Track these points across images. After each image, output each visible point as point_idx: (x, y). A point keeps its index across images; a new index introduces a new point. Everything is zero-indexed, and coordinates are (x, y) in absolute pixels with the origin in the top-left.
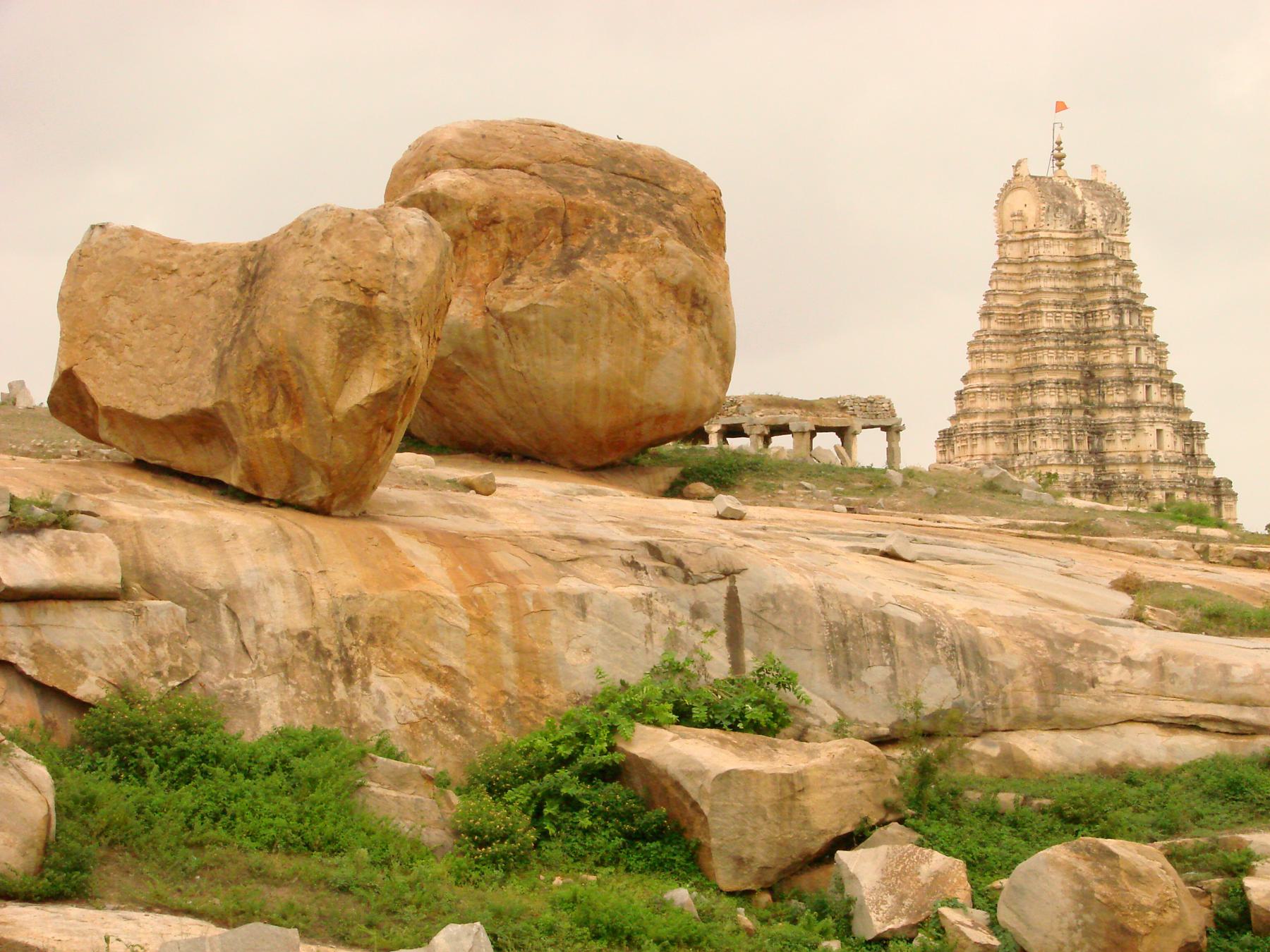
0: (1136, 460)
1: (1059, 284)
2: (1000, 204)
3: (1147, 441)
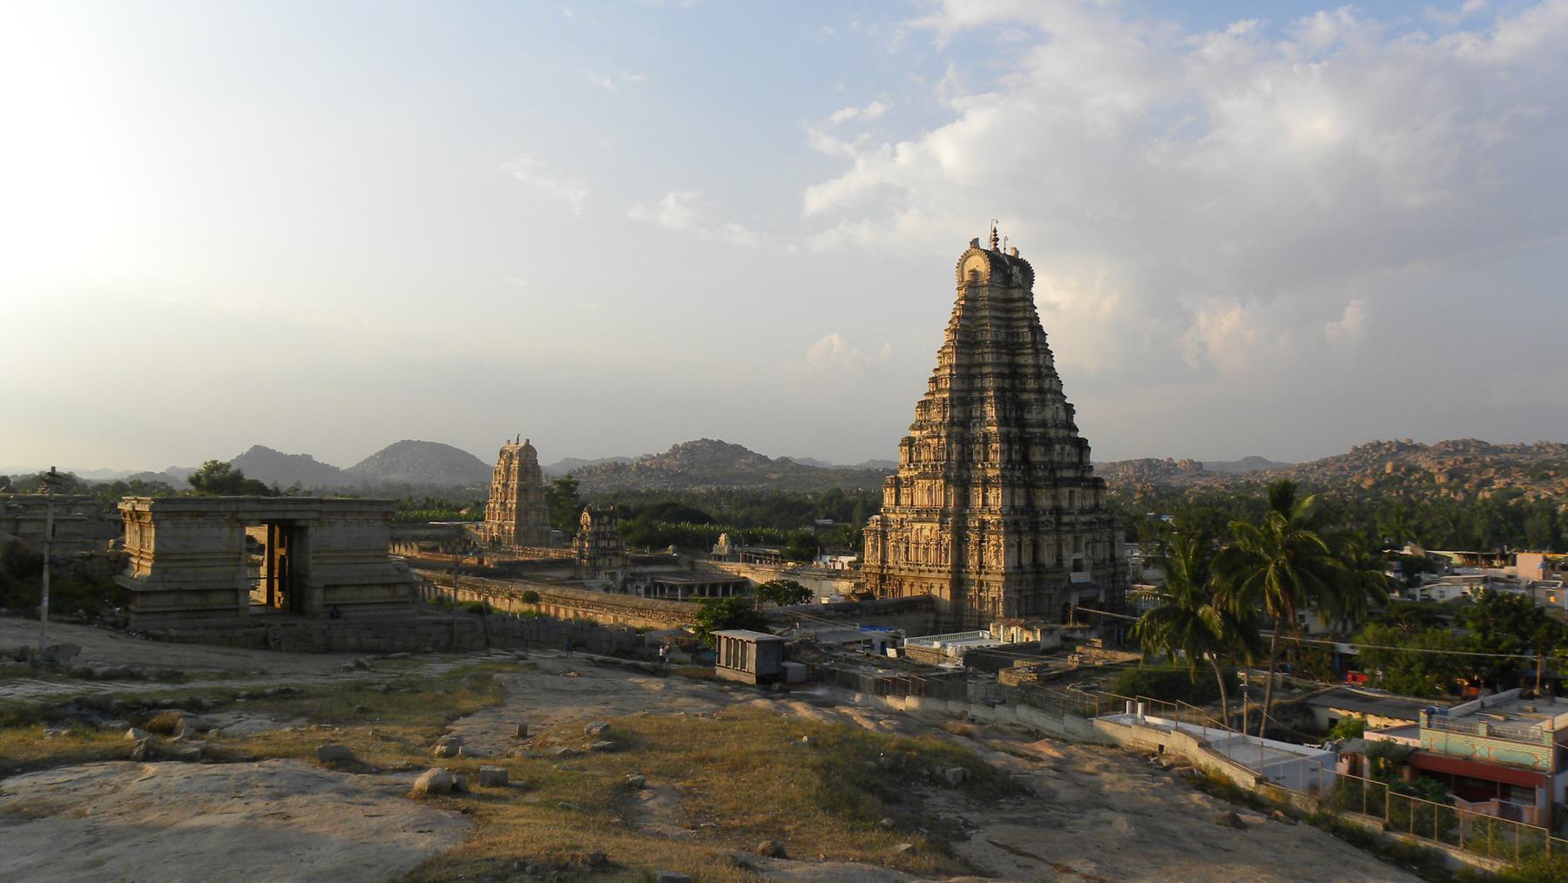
0: (1043, 424)
1: (998, 314)
2: (961, 264)
3: (1049, 413)
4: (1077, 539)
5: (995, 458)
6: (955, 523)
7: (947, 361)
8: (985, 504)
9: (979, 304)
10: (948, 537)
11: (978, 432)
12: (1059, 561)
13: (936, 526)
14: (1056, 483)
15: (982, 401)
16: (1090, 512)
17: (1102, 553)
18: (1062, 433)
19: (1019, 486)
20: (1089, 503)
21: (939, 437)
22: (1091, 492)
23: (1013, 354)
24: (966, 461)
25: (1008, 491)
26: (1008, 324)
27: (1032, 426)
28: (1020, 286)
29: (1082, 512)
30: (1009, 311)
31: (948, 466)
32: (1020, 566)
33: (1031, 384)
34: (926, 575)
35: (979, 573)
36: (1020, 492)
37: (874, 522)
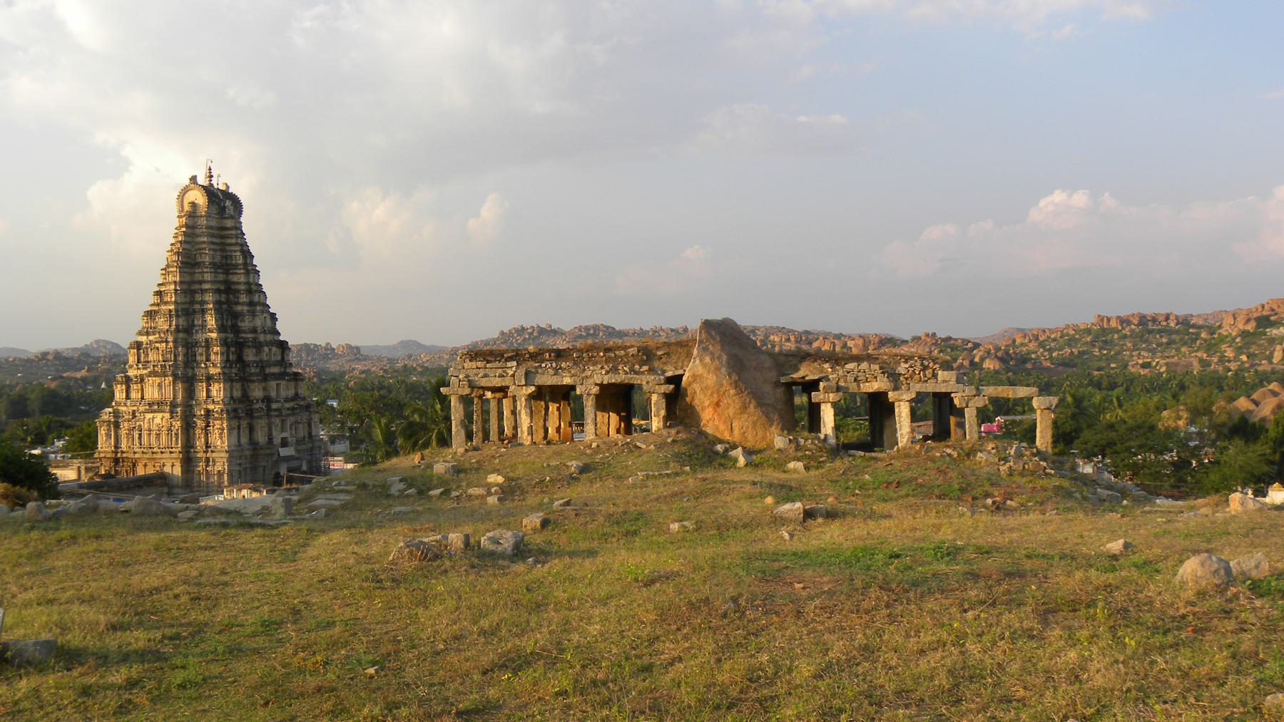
0: (254, 330)
1: (214, 240)
4: (283, 421)
5: (217, 358)
6: (184, 412)
7: (171, 278)
8: (208, 396)
9: (198, 231)
10: (177, 424)
11: (200, 337)
12: (270, 440)
13: (167, 415)
14: (266, 378)
15: (203, 312)
16: (293, 399)
17: (302, 432)
18: (269, 337)
19: (237, 381)
20: (291, 393)
21: (167, 342)
22: (292, 384)
23: (227, 273)
24: (190, 361)
25: (228, 385)
26: (223, 247)
27: (244, 332)
28: (232, 217)
29: (287, 400)
30: (222, 237)
31: (175, 366)
32: (240, 445)
33: (244, 298)
34: (159, 456)
35: (206, 452)
36: (238, 386)
37: (107, 414)
